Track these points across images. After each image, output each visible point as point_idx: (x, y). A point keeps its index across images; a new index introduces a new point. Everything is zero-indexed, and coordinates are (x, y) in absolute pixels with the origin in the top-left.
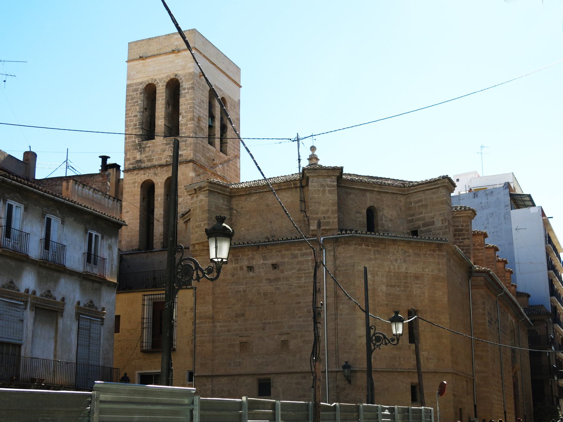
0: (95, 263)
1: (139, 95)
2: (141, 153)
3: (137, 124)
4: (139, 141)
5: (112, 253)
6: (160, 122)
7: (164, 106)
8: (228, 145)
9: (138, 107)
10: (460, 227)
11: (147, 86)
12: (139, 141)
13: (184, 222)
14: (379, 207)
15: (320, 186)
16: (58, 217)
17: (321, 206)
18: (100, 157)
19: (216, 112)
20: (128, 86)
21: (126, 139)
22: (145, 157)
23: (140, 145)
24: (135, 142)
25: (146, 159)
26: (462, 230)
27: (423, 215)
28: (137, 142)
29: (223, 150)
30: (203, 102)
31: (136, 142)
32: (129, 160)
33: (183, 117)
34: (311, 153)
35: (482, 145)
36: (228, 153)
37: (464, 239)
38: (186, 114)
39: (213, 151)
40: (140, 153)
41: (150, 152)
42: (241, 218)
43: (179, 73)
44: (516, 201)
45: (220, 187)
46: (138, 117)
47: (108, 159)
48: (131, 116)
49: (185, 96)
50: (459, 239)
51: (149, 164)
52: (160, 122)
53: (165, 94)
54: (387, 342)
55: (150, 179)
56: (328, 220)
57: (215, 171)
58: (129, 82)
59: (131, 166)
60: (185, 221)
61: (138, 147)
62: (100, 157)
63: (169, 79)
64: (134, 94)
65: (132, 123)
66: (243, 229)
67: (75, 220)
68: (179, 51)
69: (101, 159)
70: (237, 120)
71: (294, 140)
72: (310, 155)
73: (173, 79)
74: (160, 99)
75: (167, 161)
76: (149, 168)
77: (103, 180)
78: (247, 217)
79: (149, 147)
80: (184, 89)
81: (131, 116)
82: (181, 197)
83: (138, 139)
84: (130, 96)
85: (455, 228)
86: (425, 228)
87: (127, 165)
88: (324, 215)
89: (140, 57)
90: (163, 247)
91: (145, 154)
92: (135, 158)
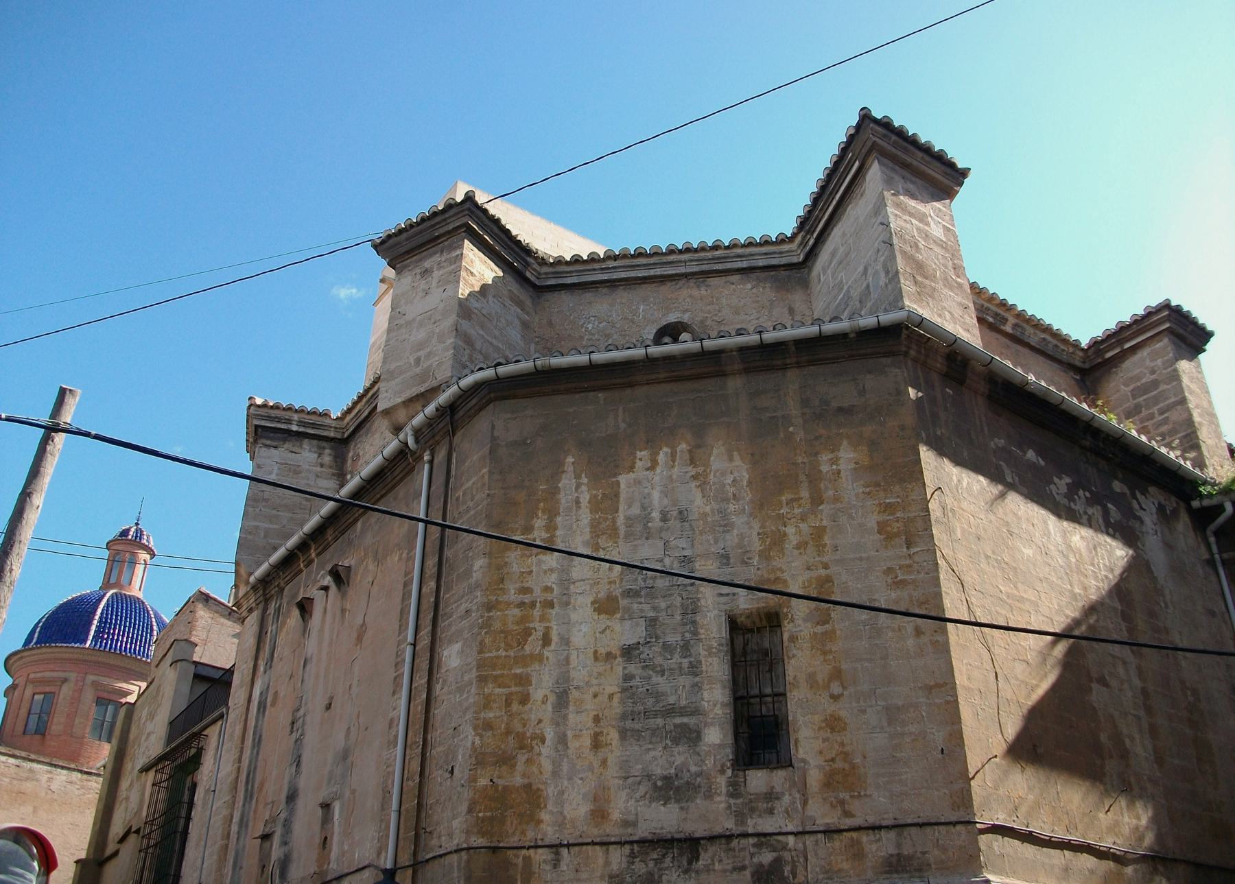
10: (1148, 378)
14: (702, 322)
15: (418, 277)
17: (415, 330)
26: (1155, 384)
37: (1169, 408)
45: (296, 417)
50: (1151, 417)
88: (419, 354)
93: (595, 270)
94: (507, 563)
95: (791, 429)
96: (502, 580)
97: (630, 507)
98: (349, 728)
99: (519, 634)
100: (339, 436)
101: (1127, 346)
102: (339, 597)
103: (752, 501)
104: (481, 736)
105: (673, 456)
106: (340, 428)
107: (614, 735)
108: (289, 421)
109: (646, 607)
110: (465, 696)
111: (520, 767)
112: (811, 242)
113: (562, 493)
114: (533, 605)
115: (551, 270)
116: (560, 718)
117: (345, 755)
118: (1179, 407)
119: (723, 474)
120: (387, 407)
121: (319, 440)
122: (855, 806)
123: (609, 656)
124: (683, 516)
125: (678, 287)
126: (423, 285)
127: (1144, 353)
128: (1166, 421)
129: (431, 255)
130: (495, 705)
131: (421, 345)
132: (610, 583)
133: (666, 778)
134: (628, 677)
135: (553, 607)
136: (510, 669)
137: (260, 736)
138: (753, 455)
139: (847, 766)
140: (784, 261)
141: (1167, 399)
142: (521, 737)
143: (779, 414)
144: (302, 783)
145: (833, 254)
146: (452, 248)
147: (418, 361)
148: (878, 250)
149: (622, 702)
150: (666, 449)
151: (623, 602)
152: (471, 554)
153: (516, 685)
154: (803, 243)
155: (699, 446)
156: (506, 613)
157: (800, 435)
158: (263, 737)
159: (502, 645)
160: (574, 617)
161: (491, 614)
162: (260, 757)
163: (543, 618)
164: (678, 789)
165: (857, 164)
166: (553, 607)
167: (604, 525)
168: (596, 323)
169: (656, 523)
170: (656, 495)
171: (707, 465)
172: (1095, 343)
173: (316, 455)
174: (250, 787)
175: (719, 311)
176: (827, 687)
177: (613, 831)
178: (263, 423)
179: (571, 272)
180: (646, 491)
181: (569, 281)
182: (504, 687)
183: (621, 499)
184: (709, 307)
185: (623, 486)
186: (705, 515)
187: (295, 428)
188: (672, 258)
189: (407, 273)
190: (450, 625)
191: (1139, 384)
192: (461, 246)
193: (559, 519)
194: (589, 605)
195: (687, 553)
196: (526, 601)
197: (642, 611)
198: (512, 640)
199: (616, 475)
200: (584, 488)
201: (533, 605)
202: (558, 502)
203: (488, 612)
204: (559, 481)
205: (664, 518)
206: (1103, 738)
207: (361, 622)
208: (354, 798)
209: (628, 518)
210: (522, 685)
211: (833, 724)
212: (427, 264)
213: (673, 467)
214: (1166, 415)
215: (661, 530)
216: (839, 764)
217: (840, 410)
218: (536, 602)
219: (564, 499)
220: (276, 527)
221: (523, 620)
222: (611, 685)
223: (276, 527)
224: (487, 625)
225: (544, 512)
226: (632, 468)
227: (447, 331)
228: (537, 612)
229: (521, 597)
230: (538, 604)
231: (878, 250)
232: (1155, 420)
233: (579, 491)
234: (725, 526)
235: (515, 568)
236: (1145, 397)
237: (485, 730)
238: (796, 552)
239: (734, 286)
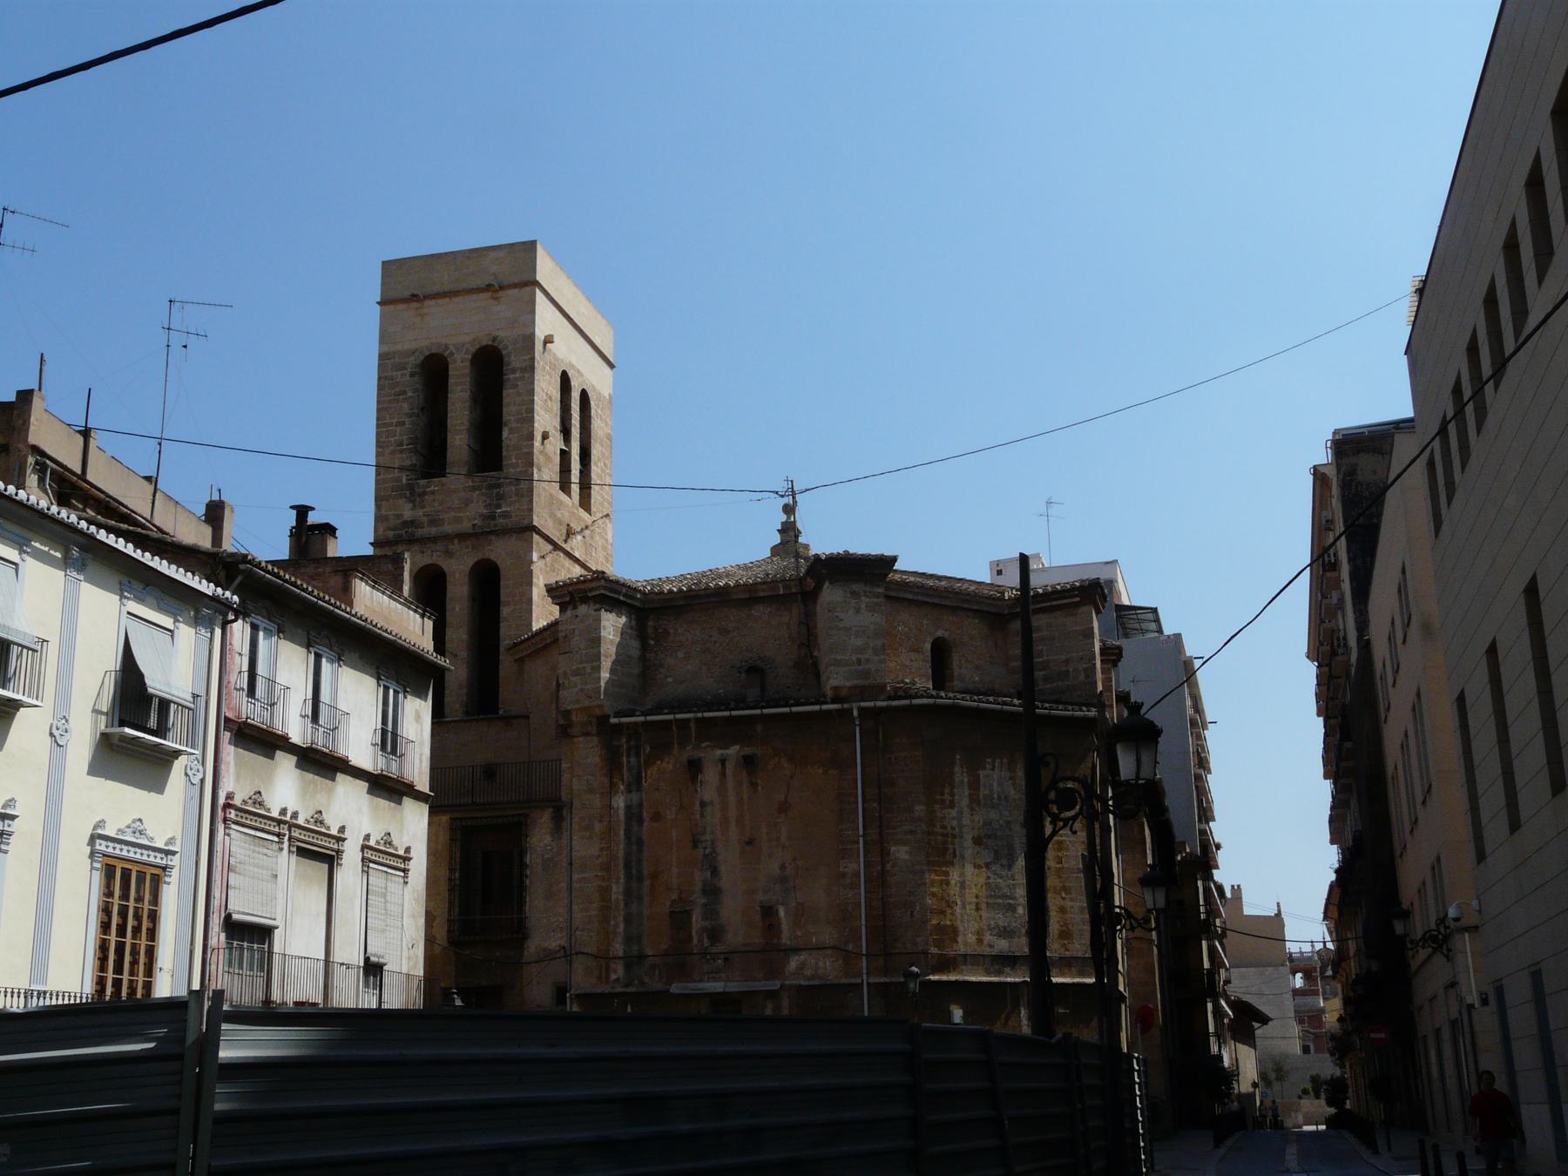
0: (394, 751)
1: (408, 378)
2: (414, 506)
3: (405, 442)
4: (408, 480)
5: (422, 731)
6: (459, 440)
7: (467, 405)
8: (592, 492)
9: (405, 405)
11: (427, 358)
12: (408, 480)
13: (515, 661)
15: (849, 595)
16: (334, 652)
18: (292, 507)
19: (573, 421)
20: (383, 357)
21: (378, 474)
22: (424, 515)
23: (411, 487)
24: (399, 480)
25: (425, 519)
27: (1045, 658)
28: (404, 481)
29: (585, 503)
30: (551, 399)
31: (401, 480)
32: (386, 520)
33: (511, 431)
34: (784, 518)
35: (1050, 499)
36: (593, 509)
38: (519, 425)
39: (568, 506)
40: (411, 505)
41: (436, 504)
42: (666, 655)
43: (501, 334)
44: (1125, 620)
46: (407, 426)
47: (310, 512)
48: (391, 424)
49: (516, 386)
51: (434, 530)
52: (459, 440)
53: (468, 379)
54: (1135, 924)
55: (435, 562)
56: (866, 667)
57: (571, 548)
58: (386, 349)
59: (391, 534)
60: (516, 657)
61: (408, 492)
62: (292, 507)
63: (478, 347)
64: (397, 375)
65: (392, 439)
66: (670, 680)
67: (361, 658)
68: (502, 288)
69: (295, 512)
70: (608, 438)
71: (783, 494)
72: (782, 523)
73: (486, 346)
74: (459, 388)
75: (474, 525)
76: (434, 539)
77: (395, 569)
78: (680, 654)
79: (433, 493)
80: (514, 371)
81: (391, 424)
82: (509, 604)
83: (407, 476)
84: (386, 378)
86: (1049, 686)
87: (381, 530)
88: (860, 656)
89: (413, 295)
90: (467, 713)
91: (423, 507)
92: (398, 516)
102: (744, 774)
105: (1002, 763)
107: (983, 906)
108: (619, 593)
111: (949, 916)
114: (947, 835)
116: (962, 895)
117: (783, 880)
122: (1070, 946)
133: (1005, 928)
134: (989, 878)
137: (640, 842)
142: (947, 902)
144: (725, 883)
147: (859, 662)
151: (985, 840)
160: (965, 845)
163: (952, 843)
164: (1009, 932)
165: (1078, 599)
174: (634, 871)
177: (987, 951)
185: (981, 776)
186: (1015, 800)
187: (622, 598)
193: (955, 790)
195: (1009, 819)
211: (1062, 910)
212: (855, 587)
216: (1064, 928)
222: (982, 880)
228: (950, 839)
229: (942, 831)
231: (1082, 659)
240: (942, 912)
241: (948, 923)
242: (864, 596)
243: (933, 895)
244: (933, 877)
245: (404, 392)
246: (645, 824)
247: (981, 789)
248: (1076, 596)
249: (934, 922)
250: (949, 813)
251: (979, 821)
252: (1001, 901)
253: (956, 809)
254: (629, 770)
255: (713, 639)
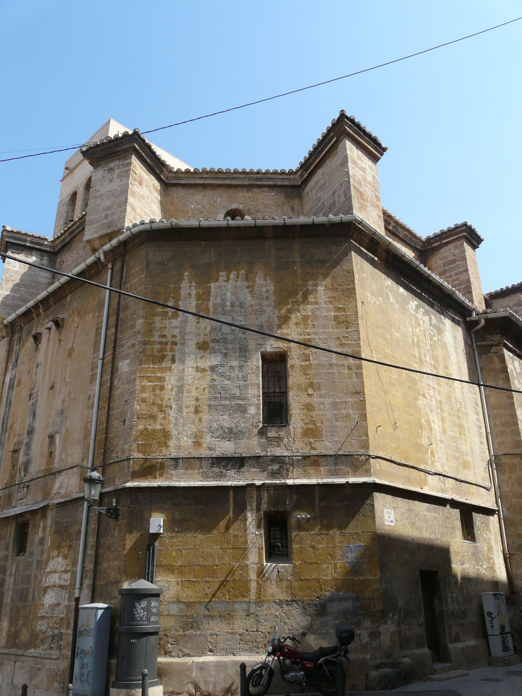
7: (80, 209)
10: (451, 258)
15: (106, 172)
17: (104, 200)
26: (454, 261)
37: (460, 273)
45: (29, 239)
50: (451, 276)
63: (87, 179)
85: (443, 262)
93: (196, 178)
94: (154, 322)
95: (295, 268)
96: (151, 330)
97: (216, 299)
98: (64, 399)
99: (159, 357)
100: (52, 250)
101: (443, 242)
102: (57, 334)
103: (275, 301)
104: (140, 405)
106: (53, 246)
108: (25, 241)
109: (222, 348)
110: (132, 385)
111: (159, 420)
112: (306, 175)
113: (182, 290)
114: (166, 343)
115: (174, 175)
116: (179, 398)
117: (62, 412)
118: (464, 273)
119: (262, 286)
120: (90, 239)
121: (41, 252)
122: (317, 445)
123: (204, 370)
124: (241, 305)
125: (237, 191)
126: (109, 176)
127: (452, 246)
128: (457, 279)
129: (113, 161)
130: (147, 391)
131: (108, 208)
132: (205, 335)
133: (230, 429)
135: (177, 345)
136: (155, 373)
137: (10, 402)
138: (276, 278)
139: (313, 427)
140: (291, 183)
141: (459, 269)
143: (290, 260)
144: (36, 425)
145: (317, 183)
146: (125, 158)
147: (106, 217)
148: (342, 184)
149: (210, 392)
150: (234, 272)
151: (211, 345)
152: (135, 317)
153: (158, 381)
154: (302, 176)
155: (250, 272)
156: (153, 346)
157: (299, 271)
158: (12, 401)
159: (151, 362)
160: (187, 350)
161: (146, 347)
162: (11, 412)
164: (235, 433)
165: (335, 139)
166: (177, 345)
167: (203, 306)
168: (196, 205)
169: (228, 307)
170: (229, 294)
171: (254, 281)
172: (429, 239)
173: (39, 260)
174: (5, 427)
175: (257, 205)
176: (306, 390)
177: (205, 453)
178: (11, 240)
179: (184, 177)
180: (224, 292)
181: (183, 182)
182: (152, 382)
183: (212, 295)
184: (252, 203)
185: (212, 289)
186: (252, 306)
187: (28, 244)
188: (235, 176)
189: (100, 169)
190: (123, 351)
191: (447, 260)
192: (130, 158)
194: (195, 345)
196: (163, 341)
197: (220, 349)
198: (156, 360)
199: (209, 283)
200: (193, 288)
201: (166, 343)
202: (180, 294)
203: (144, 346)
204: (181, 283)
205: (232, 306)
206: (423, 421)
207: (71, 347)
208: (68, 433)
209: (214, 304)
210: (161, 382)
211: (309, 407)
212: (111, 165)
213: (237, 281)
214: (458, 276)
215: (231, 311)
216: (310, 426)
217: (319, 261)
218: (168, 342)
219: (183, 293)
220: (18, 295)
221: (162, 350)
222: (205, 383)
223: (18, 295)
224: (144, 351)
225: (173, 298)
226: (217, 280)
227: (122, 202)
228: (168, 347)
230: (169, 343)
231: (342, 184)
232: (452, 278)
233: (191, 289)
234: (262, 311)
235: (158, 325)
236: (449, 267)
237: (142, 402)
238: (295, 327)
239: (265, 194)
240: (153, 417)
241: (158, 427)
242: (117, 169)
243: (144, 400)
244: (145, 383)
245: (63, 215)
246: (14, 390)
247: (212, 299)
248: (332, 138)
249: (141, 427)
250: (170, 323)
251: (205, 328)
252: (228, 402)
253: (179, 319)
254: (16, 353)
255: (80, 255)
